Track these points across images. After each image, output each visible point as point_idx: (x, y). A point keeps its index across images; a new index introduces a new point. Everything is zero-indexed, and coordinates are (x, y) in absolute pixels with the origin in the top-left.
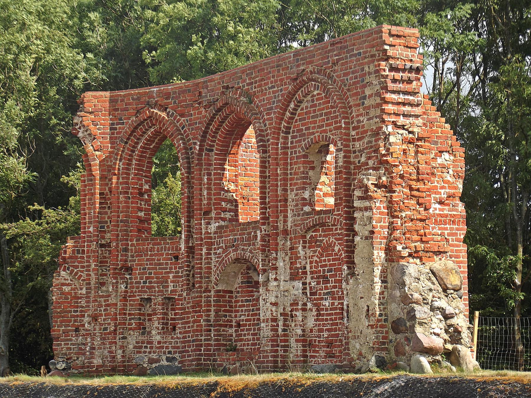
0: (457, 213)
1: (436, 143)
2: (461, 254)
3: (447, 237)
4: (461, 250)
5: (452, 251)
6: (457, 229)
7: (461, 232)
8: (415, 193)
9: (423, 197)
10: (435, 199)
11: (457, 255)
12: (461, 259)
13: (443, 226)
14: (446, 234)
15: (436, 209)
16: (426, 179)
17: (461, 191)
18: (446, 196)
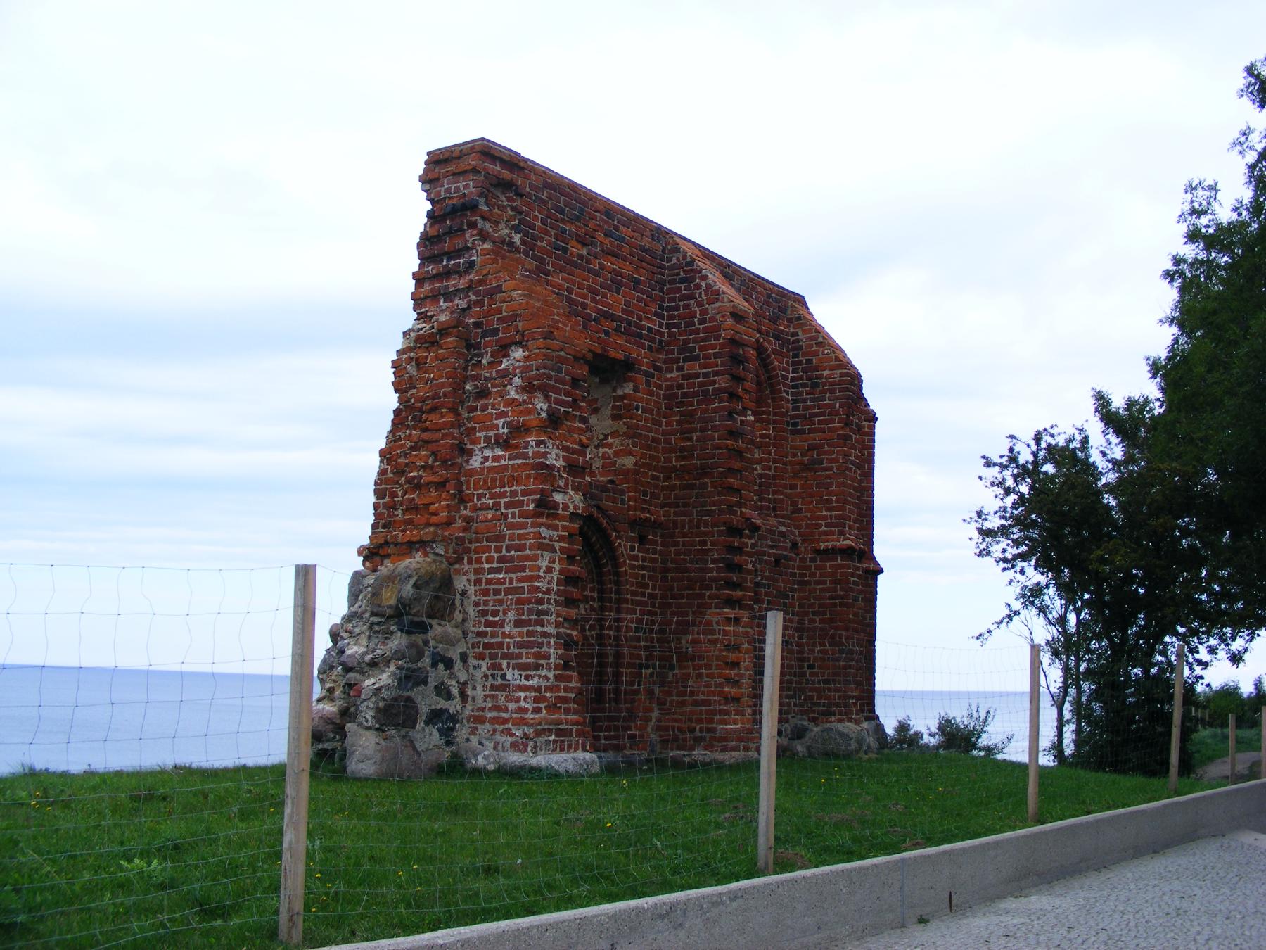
0: (524, 461)
1: (495, 332)
2: (528, 543)
3: (503, 511)
4: (528, 534)
5: (511, 537)
6: (525, 493)
7: (531, 498)
8: (425, 436)
9: (437, 441)
10: (488, 439)
11: (520, 545)
12: (528, 552)
13: (498, 490)
14: (503, 505)
15: (486, 459)
16: (443, 405)
17: (544, 415)
18: (506, 431)
